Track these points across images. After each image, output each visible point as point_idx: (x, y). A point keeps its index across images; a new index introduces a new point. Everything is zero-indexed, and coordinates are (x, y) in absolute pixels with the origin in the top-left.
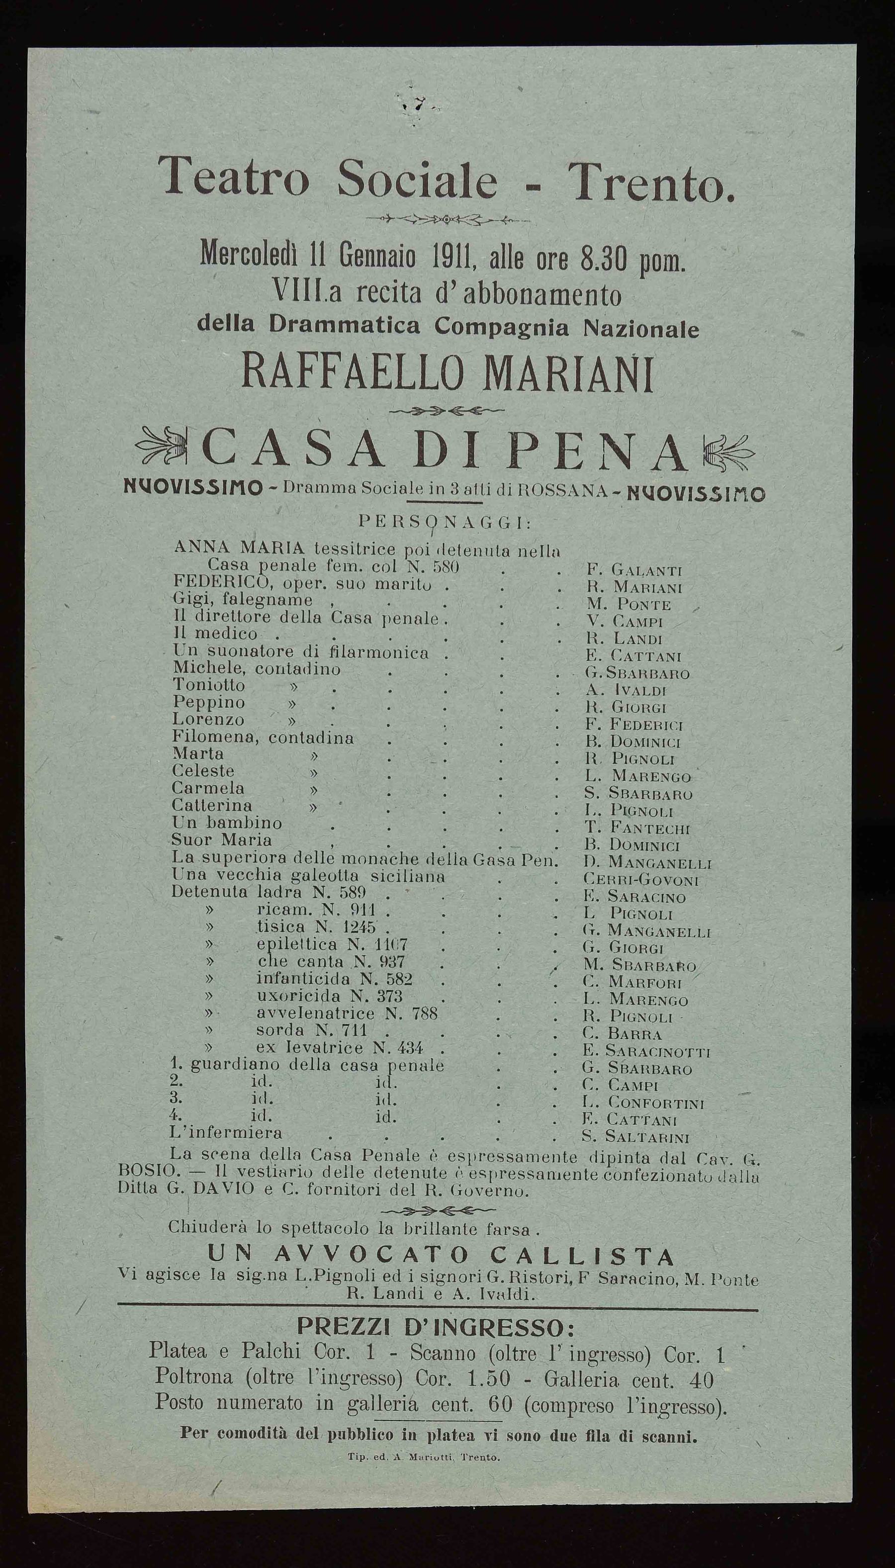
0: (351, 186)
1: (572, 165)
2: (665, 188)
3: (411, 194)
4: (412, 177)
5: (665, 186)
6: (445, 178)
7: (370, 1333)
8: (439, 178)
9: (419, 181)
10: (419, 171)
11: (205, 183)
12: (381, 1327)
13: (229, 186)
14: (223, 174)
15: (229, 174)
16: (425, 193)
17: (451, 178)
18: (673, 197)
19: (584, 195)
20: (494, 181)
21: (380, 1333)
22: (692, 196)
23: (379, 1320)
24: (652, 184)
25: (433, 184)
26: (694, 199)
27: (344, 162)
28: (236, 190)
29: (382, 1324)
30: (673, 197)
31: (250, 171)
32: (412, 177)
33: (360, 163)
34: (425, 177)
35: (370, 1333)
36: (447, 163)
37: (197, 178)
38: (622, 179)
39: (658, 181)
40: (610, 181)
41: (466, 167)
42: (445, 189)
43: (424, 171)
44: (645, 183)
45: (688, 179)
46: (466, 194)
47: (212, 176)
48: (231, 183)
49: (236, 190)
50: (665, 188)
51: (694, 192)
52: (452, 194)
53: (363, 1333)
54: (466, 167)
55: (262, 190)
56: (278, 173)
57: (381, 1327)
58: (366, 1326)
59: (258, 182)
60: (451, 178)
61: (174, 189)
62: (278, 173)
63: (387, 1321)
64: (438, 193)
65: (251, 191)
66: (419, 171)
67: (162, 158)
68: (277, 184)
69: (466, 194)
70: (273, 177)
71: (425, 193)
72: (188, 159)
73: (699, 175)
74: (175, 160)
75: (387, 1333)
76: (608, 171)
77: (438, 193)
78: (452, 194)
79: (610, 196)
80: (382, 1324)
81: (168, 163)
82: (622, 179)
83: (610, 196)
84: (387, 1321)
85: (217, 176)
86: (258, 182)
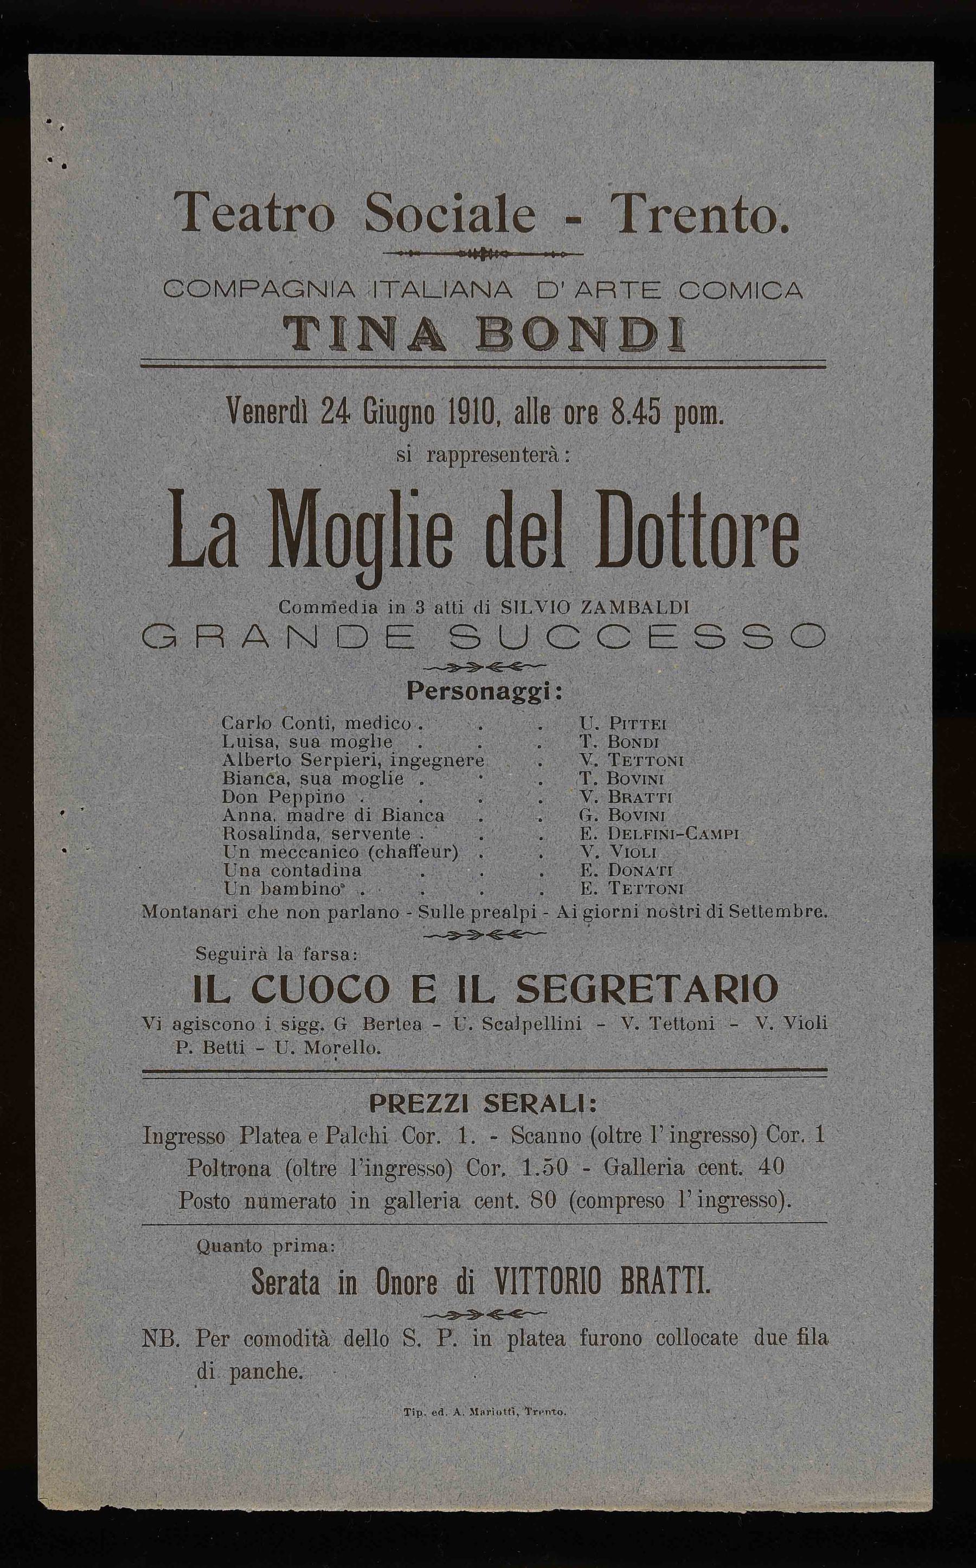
0: (379, 222)
1: (614, 196)
2: (714, 218)
3: (444, 228)
4: (444, 211)
5: (714, 216)
6: (480, 211)
7: (448, 1110)
8: (473, 211)
9: (451, 214)
10: (452, 204)
11: (225, 221)
12: (459, 1104)
13: (249, 223)
14: (243, 210)
15: (249, 211)
16: (459, 228)
17: (486, 211)
18: (723, 229)
19: (628, 228)
20: (532, 214)
21: (457, 1111)
22: (744, 227)
23: (456, 1096)
24: (700, 216)
25: (466, 218)
26: (746, 230)
27: (371, 196)
28: (257, 227)
29: (460, 1099)
30: (723, 229)
31: (272, 207)
32: (444, 211)
33: (388, 197)
34: (458, 211)
35: (448, 1110)
36: (479, 195)
37: (215, 215)
38: (668, 210)
39: (706, 212)
40: (655, 212)
41: (502, 199)
42: (479, 223)
43: (459, 203)
44: (693, 214)
45: (738, 209)
46: (502, 228)
47: (231, 212)
48: (252, 220)
49: (257, 227)
50: (714, 218)
51: (746, 223)
52: (487, 228)
53: (440, 1111)
54: (502, 199)
55: (284, 226)
56: (302, 209)
57: (459, 1104)
58: (443, 1104)
59: (281, 217)
60: (486, 211)
61: (191, 226)
62: (302, 209)
63: (465, 1096)
64: (473, 228)
65: (273, 228)
66: (452, 204)
67: (178, 194)
68: (300, 219)
69: (502, 228)
70: (296, 214)
71: (459, 228)
72: (206, 194)
73: (750, 205)
74: (191, 196)
75: (465, 1110)
76: (651, 203)
77: (473, 228)
78: (487, 228)
79: (655, 229)
80: (460, 1099)
81: (184, 199)
82: (668, 210)
83: (655, 229)
84: (465, 1096)
85: (237, 210)
86: (281, 217)
